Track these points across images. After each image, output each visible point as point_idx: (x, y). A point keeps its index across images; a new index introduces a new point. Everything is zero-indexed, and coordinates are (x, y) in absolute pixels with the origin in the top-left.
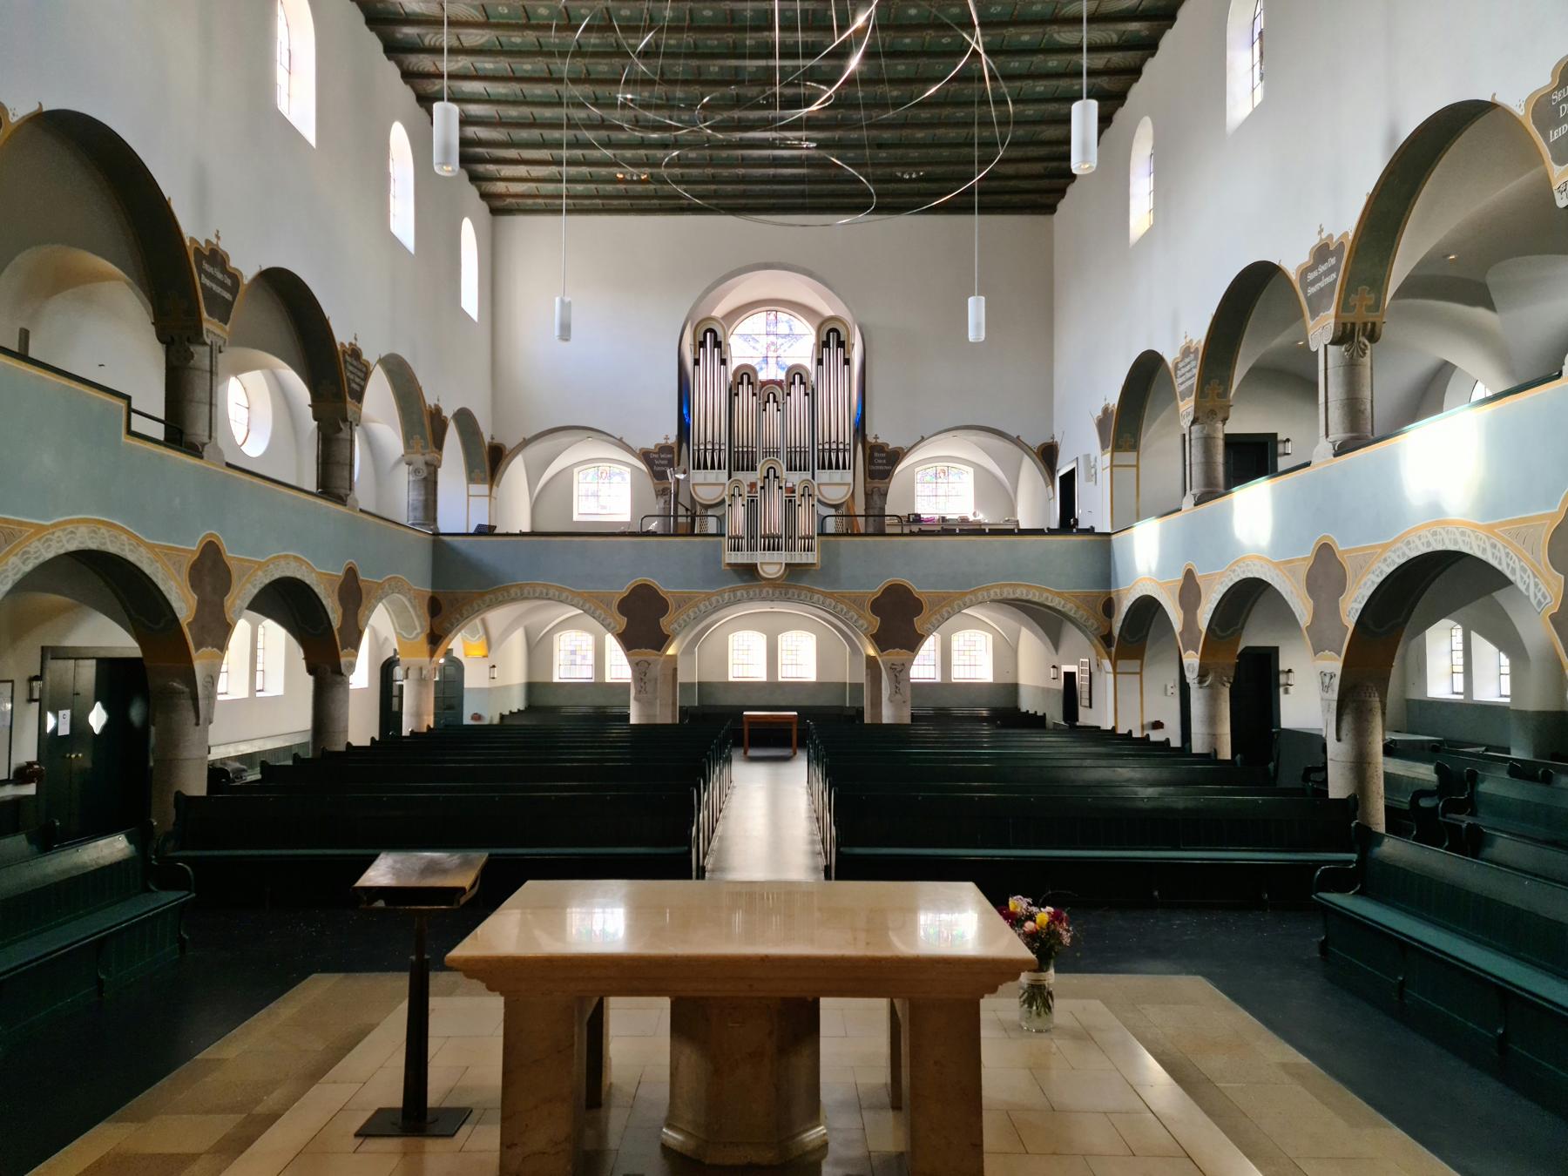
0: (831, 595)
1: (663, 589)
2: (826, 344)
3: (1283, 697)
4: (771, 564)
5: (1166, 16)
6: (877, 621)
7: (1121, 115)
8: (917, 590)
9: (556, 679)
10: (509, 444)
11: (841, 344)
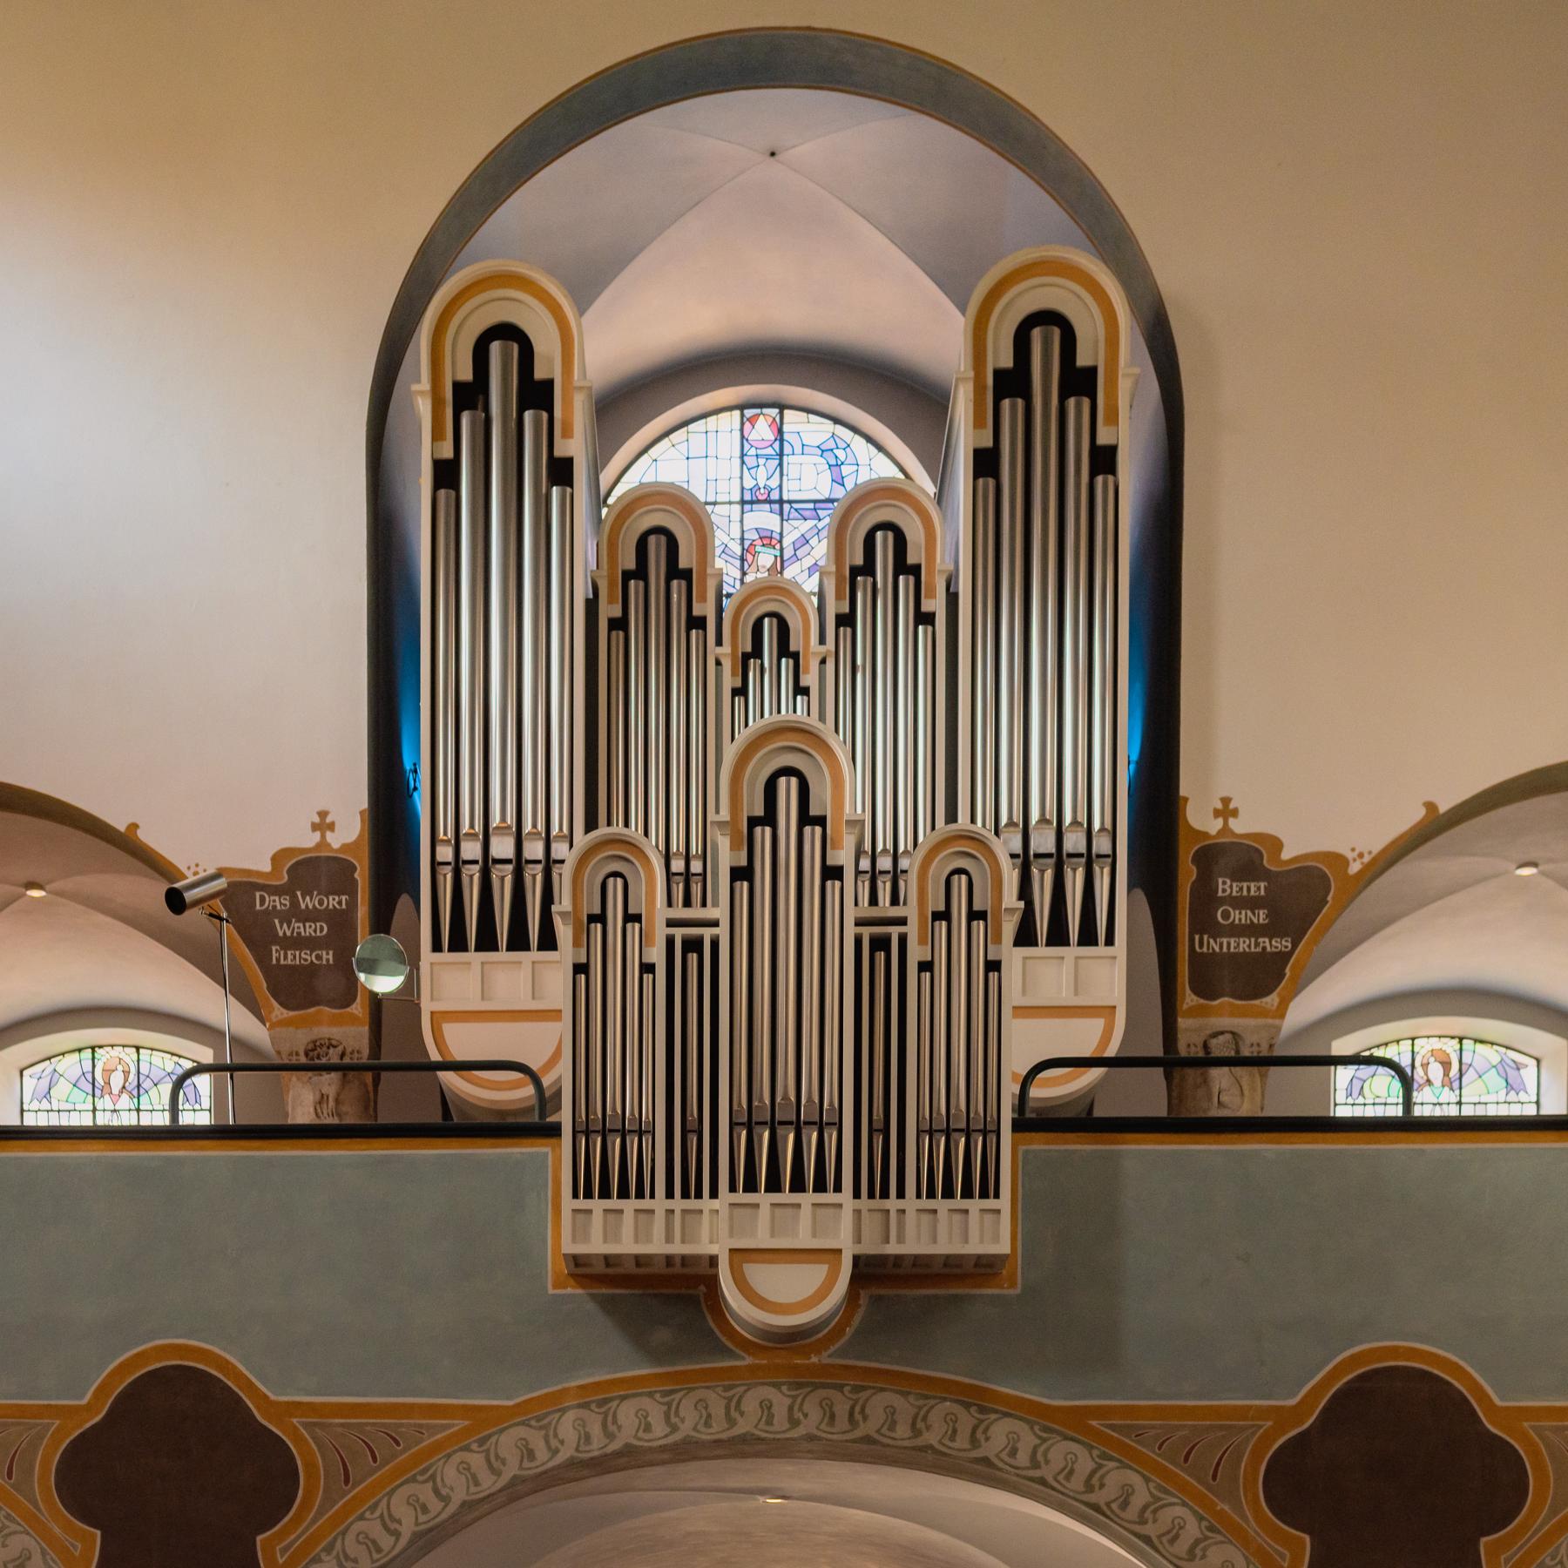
0: (1073, 1424)
8: (1500, 1394)
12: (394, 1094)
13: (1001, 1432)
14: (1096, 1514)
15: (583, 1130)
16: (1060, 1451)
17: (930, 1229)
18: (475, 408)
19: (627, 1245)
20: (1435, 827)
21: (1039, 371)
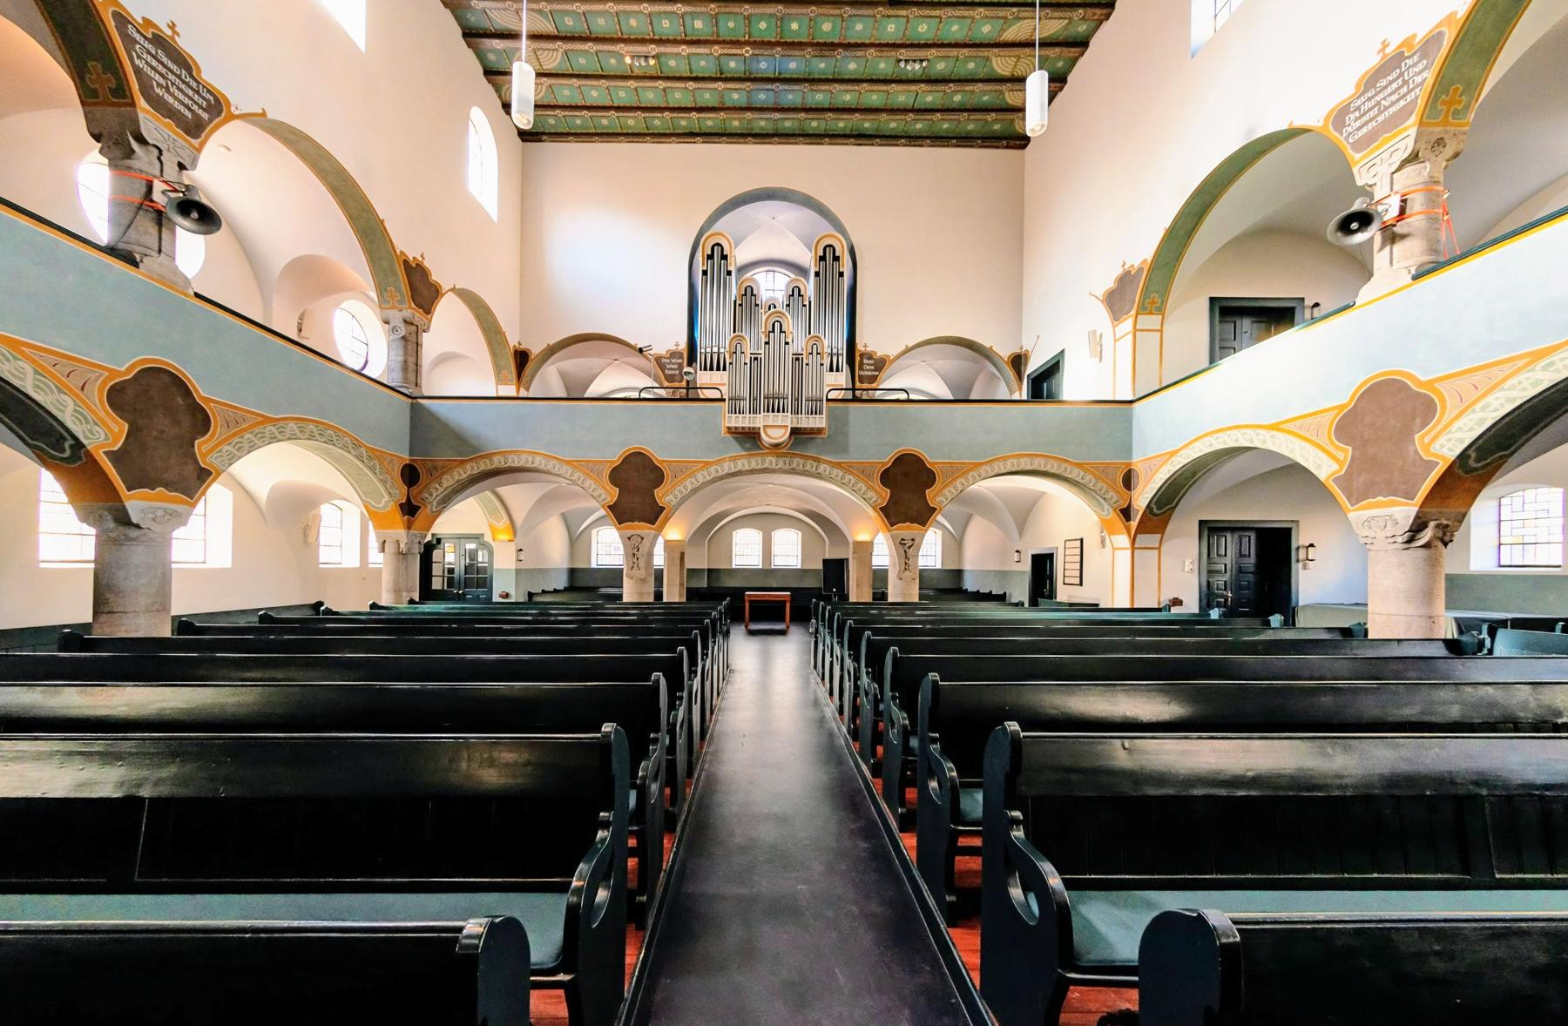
0: (839, 465)
1: (659, 455)
2: (823, 258)
4: (775, 427)
7: (1060, 95)
8: (930, 459)
9: (594, 565)
10: (535, 349)
11: (836, 259)
12: (690, 395)
13: (823, 467)
14: (843, 485)
16: (835, 471)
18: (711, 262)
19: (740, 425)
20: (908, 350)
21: (828, 256)
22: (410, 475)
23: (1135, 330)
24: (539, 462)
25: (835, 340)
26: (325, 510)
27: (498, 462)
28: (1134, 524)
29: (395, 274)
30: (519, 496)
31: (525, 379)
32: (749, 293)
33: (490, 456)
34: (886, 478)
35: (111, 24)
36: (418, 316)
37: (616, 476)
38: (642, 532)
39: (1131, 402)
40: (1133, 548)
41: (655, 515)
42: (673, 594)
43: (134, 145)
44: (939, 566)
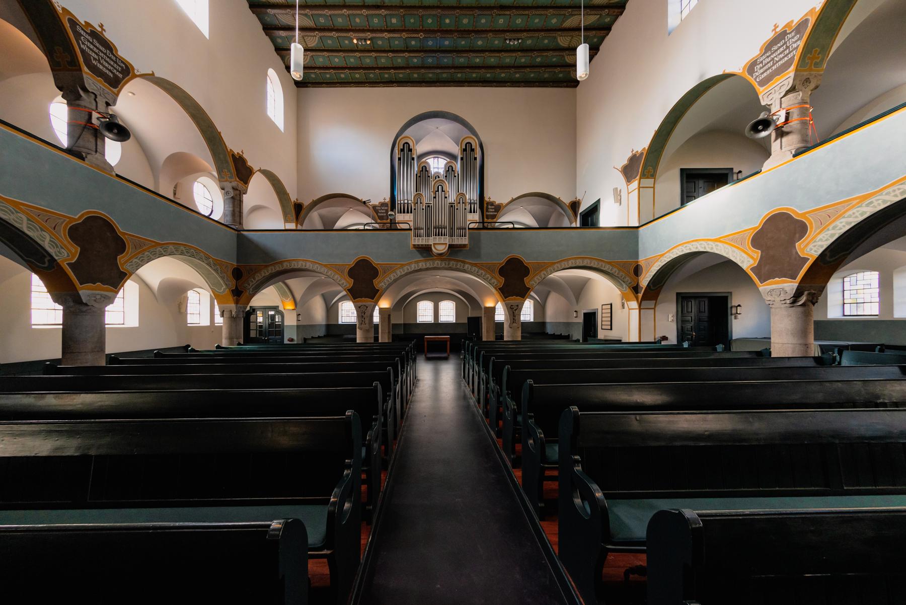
0: (475, 265)
1: (375, 261)
2: (465, 150)
3: (734, 321)
4: (440, 244)
5: (620, 7)
6: (502, 280)
7: (596, 57)
8: (526, 261)
9: (340, 322)
11: (473, 150)
12: (392, 226)
13: (467, 266)
14: (478, 276)
15: (415, 229)
16: (474, 268)
17: (458, 241)
18: (403, 154)
19: (420, 243)
20: (513, 200)
21: (468, 149)
22: (238, 274)
23: (639, 187)
24: (309, 266)
25: (472, 195)
26: (191, 294)
27: (286, 266)
28: (640, 295)
29: (227, 162)
30: (298, 285)
31: (300, 220)
32: (424, 170)
33: (281, 263)
34: (502, 271)
35: (67, 25)
36: (240, 185)
37: (352, 273)
38: (367, 304)
39: (638, 227)
40: (640, 309)
41: (374, 295)
42: (383, 338)
43: (81, 92)
44: (532, 320)
